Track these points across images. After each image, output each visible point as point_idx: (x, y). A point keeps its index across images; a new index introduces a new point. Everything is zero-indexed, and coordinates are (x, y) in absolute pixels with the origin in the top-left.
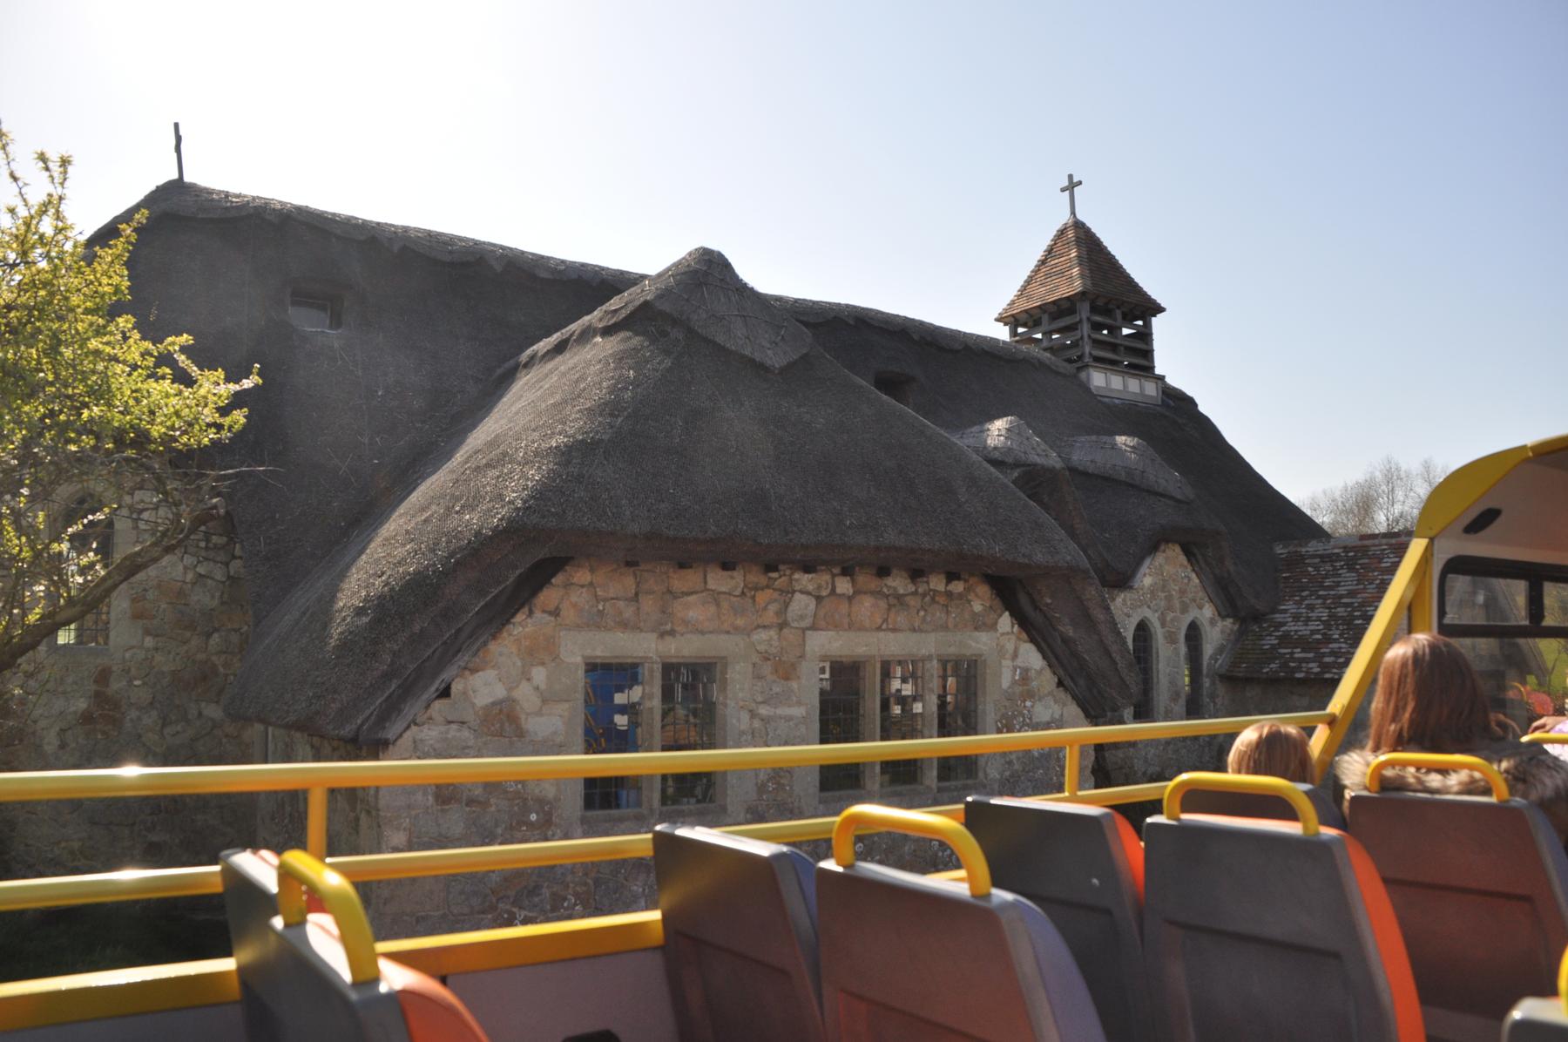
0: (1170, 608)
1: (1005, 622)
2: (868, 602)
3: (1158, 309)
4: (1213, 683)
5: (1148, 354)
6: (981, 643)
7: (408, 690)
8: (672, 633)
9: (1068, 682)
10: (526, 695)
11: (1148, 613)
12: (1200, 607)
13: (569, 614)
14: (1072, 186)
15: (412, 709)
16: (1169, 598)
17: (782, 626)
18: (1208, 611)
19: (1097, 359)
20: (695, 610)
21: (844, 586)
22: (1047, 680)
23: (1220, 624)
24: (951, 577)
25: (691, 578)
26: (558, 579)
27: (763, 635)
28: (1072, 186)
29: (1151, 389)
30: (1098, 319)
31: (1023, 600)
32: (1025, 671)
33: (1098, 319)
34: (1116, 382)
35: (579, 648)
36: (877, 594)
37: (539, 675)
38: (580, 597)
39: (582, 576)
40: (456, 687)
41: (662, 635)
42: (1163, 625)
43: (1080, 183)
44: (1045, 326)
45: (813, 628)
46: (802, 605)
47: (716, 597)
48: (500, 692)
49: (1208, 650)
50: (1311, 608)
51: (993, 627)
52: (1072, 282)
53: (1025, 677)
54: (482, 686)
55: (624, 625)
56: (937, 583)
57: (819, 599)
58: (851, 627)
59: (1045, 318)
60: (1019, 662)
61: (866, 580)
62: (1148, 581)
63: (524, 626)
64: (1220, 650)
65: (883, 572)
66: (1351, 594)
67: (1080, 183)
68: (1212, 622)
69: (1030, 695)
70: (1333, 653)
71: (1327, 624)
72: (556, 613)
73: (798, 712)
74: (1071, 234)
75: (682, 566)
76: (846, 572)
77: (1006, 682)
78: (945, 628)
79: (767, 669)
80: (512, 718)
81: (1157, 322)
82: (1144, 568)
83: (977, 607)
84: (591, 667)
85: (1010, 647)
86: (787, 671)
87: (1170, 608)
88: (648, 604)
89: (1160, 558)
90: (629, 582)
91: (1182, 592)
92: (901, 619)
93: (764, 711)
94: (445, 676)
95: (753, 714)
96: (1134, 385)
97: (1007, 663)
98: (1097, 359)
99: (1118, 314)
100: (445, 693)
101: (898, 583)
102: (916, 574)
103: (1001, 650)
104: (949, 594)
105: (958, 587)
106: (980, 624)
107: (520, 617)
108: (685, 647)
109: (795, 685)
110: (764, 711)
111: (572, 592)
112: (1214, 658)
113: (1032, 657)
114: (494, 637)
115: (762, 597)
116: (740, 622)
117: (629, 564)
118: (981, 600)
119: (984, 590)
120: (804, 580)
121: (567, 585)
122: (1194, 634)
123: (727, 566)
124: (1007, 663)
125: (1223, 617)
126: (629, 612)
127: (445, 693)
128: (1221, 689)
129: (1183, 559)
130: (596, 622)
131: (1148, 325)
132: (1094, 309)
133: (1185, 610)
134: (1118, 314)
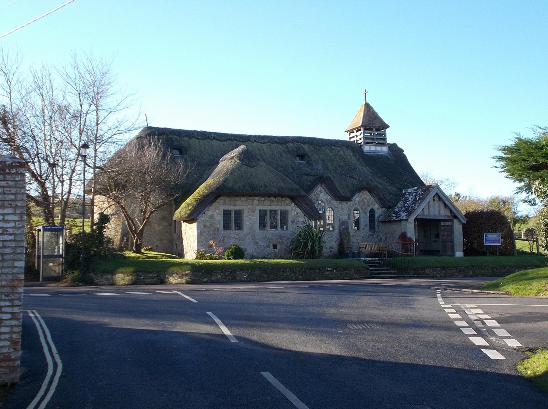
0: (364, 205)
3: (387, 127)
4: (378, 223)
5: (385, 139)
6: (288, 208)
7: (200, 213)
10: (215, 214)
13: (221, 203)
15: (200, 215)
16: (364, 203)
19: (367, 143)
20: (239, 203)
21: (263, 199)
22: (302, 214)
32: (297, 213)
35: (222, 208)
37: (217, 211)
38: (222, 201)
39: (222, 198)
49: (377, 215)
53: (297, 213)
54: (209, 213)
62: (357, 199)
63: (215, 205)
68: (378, 209)
69: (298, 217)
81: (387, 130)
82: (356, 195)
84: (224, 211)
85: (294, 209)
86: (253, 211)
87: (364, 205)
88: (232, 202)
89: (361, 194)
90: (229, 199)
91: (368, 202)
92: (273, 204)
96: (379, 148)
98: (367, 143)
99: (374, 130)
101: (272, 198)
103: (292, 209)
108: (237, 208)
111: (221, 200)
113: (299, 211)
118: (288, 201)
119: (289, 200)
120: (256, 198)
122: (372, 212)
128: (381, 224)
130: (225, 204)
131: (385, 131)
133: (369, 206)
134: (374, 130)
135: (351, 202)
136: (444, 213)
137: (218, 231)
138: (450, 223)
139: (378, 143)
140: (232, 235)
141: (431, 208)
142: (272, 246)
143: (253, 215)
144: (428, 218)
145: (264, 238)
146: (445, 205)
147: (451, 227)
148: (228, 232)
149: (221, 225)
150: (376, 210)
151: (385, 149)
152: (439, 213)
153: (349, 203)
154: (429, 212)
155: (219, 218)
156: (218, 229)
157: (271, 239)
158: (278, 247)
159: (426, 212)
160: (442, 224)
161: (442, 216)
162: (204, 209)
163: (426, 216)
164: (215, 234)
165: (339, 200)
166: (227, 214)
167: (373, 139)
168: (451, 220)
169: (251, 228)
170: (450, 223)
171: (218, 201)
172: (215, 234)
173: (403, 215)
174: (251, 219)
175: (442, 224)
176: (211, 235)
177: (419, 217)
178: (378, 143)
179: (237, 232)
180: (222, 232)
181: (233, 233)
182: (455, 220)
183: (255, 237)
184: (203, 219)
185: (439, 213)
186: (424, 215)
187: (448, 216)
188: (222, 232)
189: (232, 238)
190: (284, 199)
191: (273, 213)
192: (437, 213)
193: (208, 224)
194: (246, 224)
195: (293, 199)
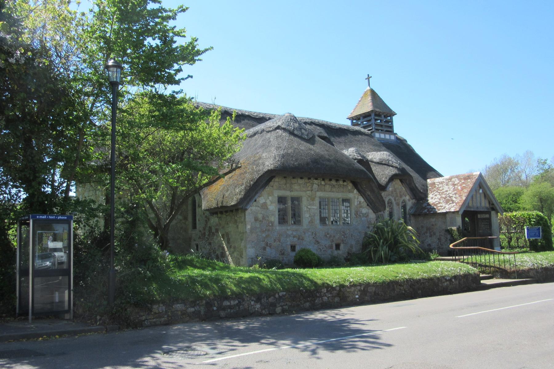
0: (397, 196)
1: (355, 191)
2: (328, 186)
4: (410, 217)
5: (392, 127)
6: (350, 196)
7: (250, 200)
10: (268, 202)
11: (391, 197)
12: (405, 196)
13: (275, 187)
14: (369, 78)
15: (251, 204)
16: (396, 194)
17: (312, 190)
18: (408, 197)
19: (377, 130)
20: (296, 187)
21: (323, 183)
22: (365, 204)
23: (411, 201)
24: (344, 181)
25: (294, 181)
26: (273, 180)
27: (308, 192)
28: (369, 78)
29: (393, 137)
30: (377, 118)
31: (359, 186)
32: (360, 202)
33: (377, 118)
34: (382, 136)
35: (277, 193)
36: (330, 185)
37: (270, 198)
38: (276, 184)
39: (276, 179)
42: (395, 200)
44: (361, 120)
45: (318, 191)
46: (315, 186)
47: (300, 185)
48: (264, 201)
49: (408, 208)
50: (436, 195)
51: (353, 192)
52: (368, 107)
54: (261, 200)
55: (284, 189)
56: (341, 182)
58: (324, 191)
59: (361, 118)
61: (327, 181)
62: (390, 189)
63: (268, 189)
64: (412, 208)
65: (330, 180)
66: (447, 191)
68: (409, 200)
69: (361, 207)
70: (441, 206)
71: (440, 199)
72: (273, 187)
73: (315, 207)
74: (369, 93)
75: (294, 178)
76: (323, 180)
77: (356, 204)
78: (343, 192)
79: (309, 199)
81: (394, 118)
83: (349, 188)
85: (357, 196)
86: (313, 199)
87: (397, 196)
88: (288, 185)
89: (394, 183)
91: (400, 192)
92: (334, 190)
93: (309, 207)
94: (256, 197)
95: (307, 208)
96: (387, 136)
97: (356, 200)
98: (377, 130)
99: (383, 116)
102: (337, 180)
103: (355, 197)
104: (344, 185)
105: (345, 183)
106: (350, 192)
107: (267, 187)
108: (295, 194)
110: (309, 207)
112: (410, 210)
113: (362, 199)
115: (308, 184)
117: (285, 177)
118: (350, 186)
119: (351, 184)
120: (316, 181)
123: (301, 178)
124: (356, 200)
125: (412, 199)
127: (255, 201)
128: (412, 218)
129: (400, 183)
130: (279, 188)
131: (392, 119)
132: (376, 115)
133: (401, 196)
134: (383, 116)
136: (484, 204)
137: (273, 225)
138: (487, 216)
139: (386, 131)
140: (290, 233)
143: (313, 205)
144: (472, 210)
145: (326, 236)
146: (485, 195)
147: (489, 220)
148: (284, 228)
149: (275, 219)
151: (393, 137)
152: (480, 204)
154: (472, 203)
155: (273, 207)
156: (272, 223)
157: (334, 236)
158: (342, 246)
160: (479, 216)
162: (255, 195)
164: (269, 230)
166: (281, 200)
167: (381, 126)
168: (489, 213)
169: (311, 222)
170: (487, 216)
172: (269, 230)
173: (447, 206)
174: (309, 210)
175: (479, 216)
176: (263, 232)
178: (386, 131)
179: (295, 227)
180: (278, 228)
181: (290, 229)
182: (493, 213)
184: (254, 208)
185: (480, 204)
187: (487, 208)
189: (290, 236)
192: (479, 205)
193: (260, 216)
194: (306, 217)
195: (356, 185)
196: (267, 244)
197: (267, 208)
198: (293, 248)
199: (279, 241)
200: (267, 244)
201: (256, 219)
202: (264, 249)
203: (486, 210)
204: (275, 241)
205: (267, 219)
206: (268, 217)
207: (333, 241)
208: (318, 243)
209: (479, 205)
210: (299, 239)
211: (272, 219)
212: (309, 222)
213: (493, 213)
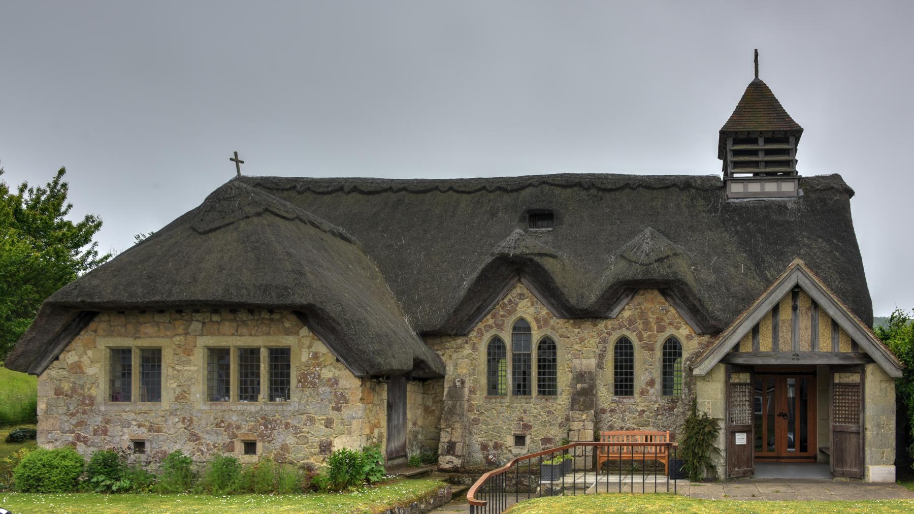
1: (305, 331)
8: (139, 338)
9: (340, 358)
10: (85, 359)
11: (627, 333)
16: (646, 323)
17: (187, 334)
20: (149, 329)
26: (96, 319)
27: (178, 338)
32: (316, 356)
37: (90, 353)
40: (61, 357)
41: (136, 338)
43: (236, 154)
45: (202, 335)
47: (158, 324)
48: (76, 358)
51: (297, 333)
53: (316, 356)
54: (70, 357)
55: (121, 335)
57: (204, 323)
60: (313, 349)
63: (85, 336)
67: (236, 154)
69: (319, 365)
72: (96, 331)
77: (304, 358)
78: (268, 334)
80: (80, 368)
86: (188, 352)
93: (178, 368)
94: (56, 352)
100: (57, 358)
106: (287, 332)
107: (82, 333)
109: (192, 358)
110: (178, 368)
111: (100, 324)
113: (321, 348)
114: (72, 339)
115: (180, 322)
116: (168, 333)
119: (293, 317)
121: (100, 321)
126: (123, 330)
127: (57, 358)
130: (110, 334)
135: (609, 322)
137: (92, 404)
141: (785, 333)
142: (239, 447)
143: (189, 363)
144: (773, 362)
149: (100, 390)
150: (684, 342)
152: (813, 345)
153: (602, 325)
159: (765, 343)
161: (822, 355)
163: (766, 355)
165: (572, 319)
166: (121, 356)
171: (92, 325)
176: (73, 415)
177: (740, 361)
180: (103, 408)
183: (191, 421)
185: (813, 345)
186: (756, 353)
187: (845, 356)
188: (103, 408)
190: (276, 316)
191: (249, 356)
193: (66, 386)
194: (169, 386)
196: (78, 438)
197: (83, 373)
198: (139, 445)
199: (105, 432)
200: (78, 438)
201: (58, 392)
202: (74, 444)
203: (835, 361)
204: (95, 432)
205: (80, 391)
206: (82, 387)
207: (235, 436)
208: (199, 439)
209: (804, 347)
210: (150, 430)
211: (93, 392)
212: (177, 398)
213: (870, 369)
